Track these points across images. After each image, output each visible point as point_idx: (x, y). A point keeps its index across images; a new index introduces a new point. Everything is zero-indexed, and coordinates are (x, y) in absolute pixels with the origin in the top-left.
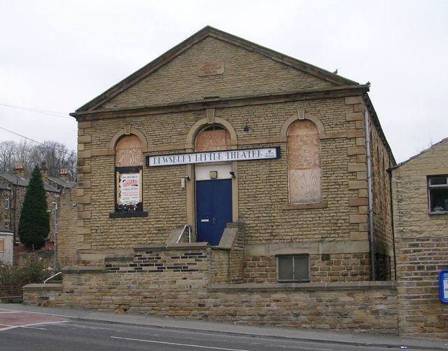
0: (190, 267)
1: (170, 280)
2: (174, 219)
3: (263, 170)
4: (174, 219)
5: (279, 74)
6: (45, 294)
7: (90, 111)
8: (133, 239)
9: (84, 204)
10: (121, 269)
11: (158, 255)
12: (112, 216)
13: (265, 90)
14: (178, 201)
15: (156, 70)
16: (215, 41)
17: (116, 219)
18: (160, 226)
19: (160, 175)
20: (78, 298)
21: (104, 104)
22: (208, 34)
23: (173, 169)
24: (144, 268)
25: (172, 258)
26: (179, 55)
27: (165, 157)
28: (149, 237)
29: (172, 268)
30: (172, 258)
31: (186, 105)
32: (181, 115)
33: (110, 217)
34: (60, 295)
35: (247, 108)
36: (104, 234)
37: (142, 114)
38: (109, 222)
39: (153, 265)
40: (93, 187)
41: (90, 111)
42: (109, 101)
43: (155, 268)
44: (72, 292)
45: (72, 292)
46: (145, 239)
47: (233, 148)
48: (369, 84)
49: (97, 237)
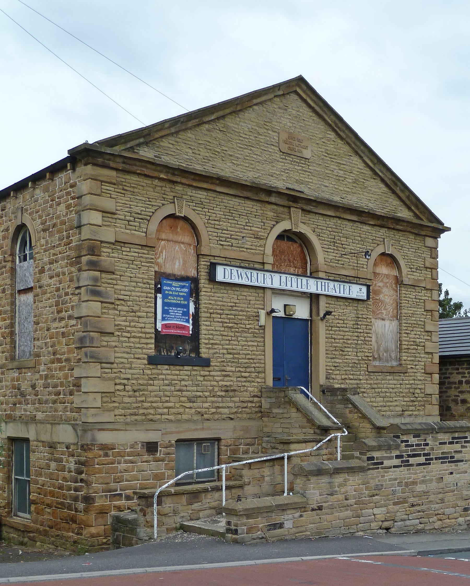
0: (457, 456)
1: (438, 476)
2: (247, 374)
3: (349, 312)
4: (247, 374)
5: (368, 183)
6: (276, 518)
7: (117, 149)
8: (188, 405)
9: (103, 333)
10: (387, 463)
11: (425, 440)
12: (152, 361)
13: (353, 200)
14: (253, 346)
15: (223, 117)
16: (299, 102)
17: (159, 367)
18: (228, 384)
19: (229, 297)
20: (329, 517)
21: (139, 145)
22: (298, 87)
23: (246, 292)
24: (412, 460)
25: (441, 444)
26: (256, 105)
27: (240, 270)
28: (213, 402)
29: (440, 458)
30: (441, 444)
31: (269, 191)
32: (257, 206)
33: (149, 363)
34: (301, 516)
35: (335, 220)
36: (137, 394)
37: (205, 185)
38: (149, 372)
39: (419, 455)
40: (118, 302)
41: (117, 149)
42: (146, 144)
43: (422, 459)
44: (320, 508)
45: (320, 508)
46: (206, 405)
47: (257, 266)
48: (449, 229)
49: (127, 400)
